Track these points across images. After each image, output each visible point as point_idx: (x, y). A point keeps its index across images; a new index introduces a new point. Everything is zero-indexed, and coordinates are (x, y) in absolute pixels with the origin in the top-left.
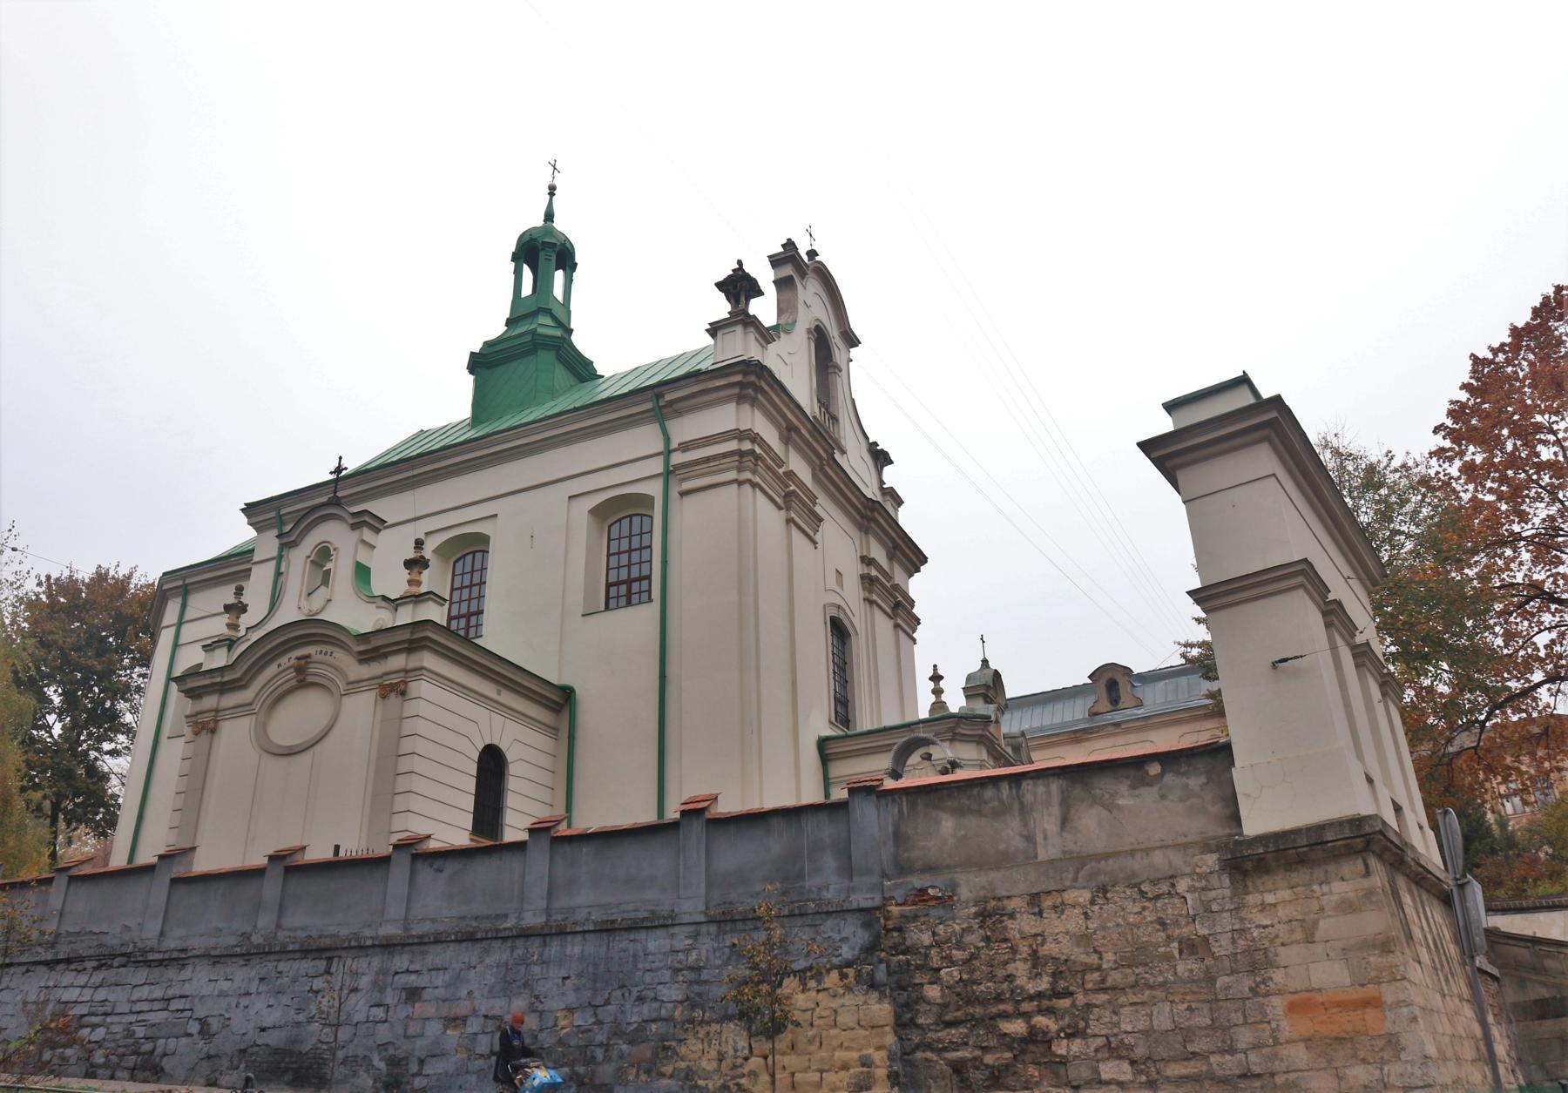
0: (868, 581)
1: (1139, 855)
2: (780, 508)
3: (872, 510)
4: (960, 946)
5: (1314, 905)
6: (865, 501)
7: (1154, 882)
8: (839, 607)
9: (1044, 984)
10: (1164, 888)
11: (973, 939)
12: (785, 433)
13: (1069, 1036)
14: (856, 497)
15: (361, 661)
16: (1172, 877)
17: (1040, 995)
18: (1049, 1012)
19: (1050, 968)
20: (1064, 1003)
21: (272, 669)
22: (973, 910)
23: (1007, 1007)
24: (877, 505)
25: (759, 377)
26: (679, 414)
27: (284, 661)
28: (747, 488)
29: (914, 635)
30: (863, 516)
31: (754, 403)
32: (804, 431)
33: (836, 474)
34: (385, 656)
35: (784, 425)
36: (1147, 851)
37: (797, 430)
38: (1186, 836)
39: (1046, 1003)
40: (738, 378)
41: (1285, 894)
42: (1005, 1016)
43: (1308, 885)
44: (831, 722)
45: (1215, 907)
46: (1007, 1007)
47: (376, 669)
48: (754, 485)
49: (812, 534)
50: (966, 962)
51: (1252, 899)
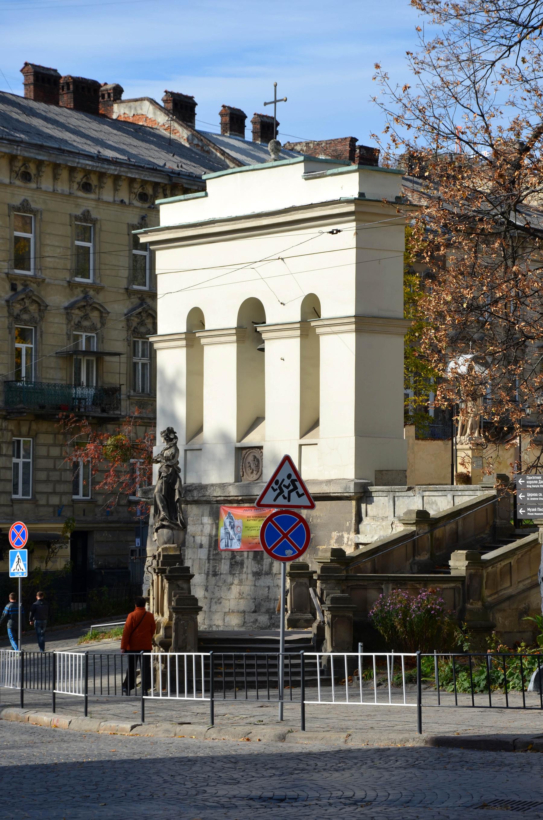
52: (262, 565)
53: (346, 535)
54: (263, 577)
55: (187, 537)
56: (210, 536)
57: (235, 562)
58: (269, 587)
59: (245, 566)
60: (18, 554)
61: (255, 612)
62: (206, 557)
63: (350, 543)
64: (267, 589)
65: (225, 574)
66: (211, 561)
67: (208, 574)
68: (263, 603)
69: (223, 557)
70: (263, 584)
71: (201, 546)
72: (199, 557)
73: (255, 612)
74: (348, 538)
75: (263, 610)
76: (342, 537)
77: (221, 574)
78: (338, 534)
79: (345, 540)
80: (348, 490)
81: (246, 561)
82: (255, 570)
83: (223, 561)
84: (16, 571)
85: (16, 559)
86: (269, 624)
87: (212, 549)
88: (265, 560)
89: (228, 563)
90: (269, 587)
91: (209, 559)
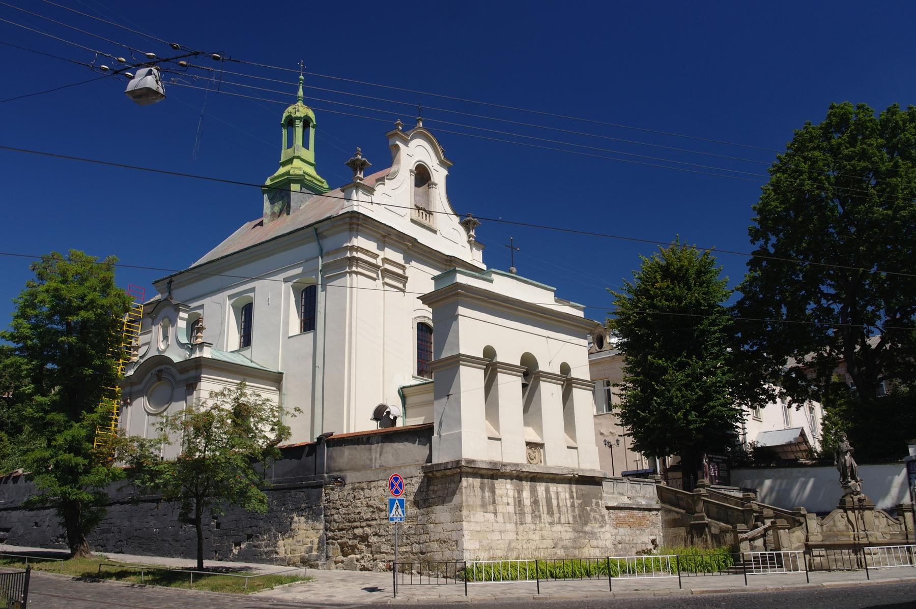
1: (403, 468)
2: (374, 279)
4: (346, 500)
5: (446, 492)
7: (406, 478)
8: (424, 317)
9: (368, 516)
10: (409, 481)
11: (350, 497)
12: (382, 238)
13: (374, 535)
15: (181, 373)
16: (412, 477)
17: (367, 520)
18: (369, 526)
19: (372, 509)
20: (374, 523)
21: (149, 375)
22: (351, 487)
23: (357, 524)
26: (325, 237)
27: (153, 371)
28: (354, 275)
30: (446, 265)
34: (188, 371)
35: (379, 236)
36: (405, 467)
38: (418, 461)
39: (368, 522)
41: (440, 486)
42: (357, 527)
43: (445, 484)
44: (413, 377)
45: (422, 490)
46: (357, 524)
47: (184, 376)
48: (357, 273)
49: (401, 286)
50: (347, 506)
51: (431, 488)
52: (554, 518)
53: (600, 502)
58: (561, 532)
59: (542, 518)
60: (397, 501)
61: (554, 548)
62: (513, 512)
65: (530, 523)
67: (516, 524)
68: (558, 542)
70: (557, 530)
71: (508, 504)
73: (554, 548)
75: (560, 546)
76: (598, 502)
79: (600, 504)
81: (542, 515)
82: (549, 521)
84: (394, 516)
85: (395, 506)
87: (517, 506)
89: (530, 516)
90: (561, 532)
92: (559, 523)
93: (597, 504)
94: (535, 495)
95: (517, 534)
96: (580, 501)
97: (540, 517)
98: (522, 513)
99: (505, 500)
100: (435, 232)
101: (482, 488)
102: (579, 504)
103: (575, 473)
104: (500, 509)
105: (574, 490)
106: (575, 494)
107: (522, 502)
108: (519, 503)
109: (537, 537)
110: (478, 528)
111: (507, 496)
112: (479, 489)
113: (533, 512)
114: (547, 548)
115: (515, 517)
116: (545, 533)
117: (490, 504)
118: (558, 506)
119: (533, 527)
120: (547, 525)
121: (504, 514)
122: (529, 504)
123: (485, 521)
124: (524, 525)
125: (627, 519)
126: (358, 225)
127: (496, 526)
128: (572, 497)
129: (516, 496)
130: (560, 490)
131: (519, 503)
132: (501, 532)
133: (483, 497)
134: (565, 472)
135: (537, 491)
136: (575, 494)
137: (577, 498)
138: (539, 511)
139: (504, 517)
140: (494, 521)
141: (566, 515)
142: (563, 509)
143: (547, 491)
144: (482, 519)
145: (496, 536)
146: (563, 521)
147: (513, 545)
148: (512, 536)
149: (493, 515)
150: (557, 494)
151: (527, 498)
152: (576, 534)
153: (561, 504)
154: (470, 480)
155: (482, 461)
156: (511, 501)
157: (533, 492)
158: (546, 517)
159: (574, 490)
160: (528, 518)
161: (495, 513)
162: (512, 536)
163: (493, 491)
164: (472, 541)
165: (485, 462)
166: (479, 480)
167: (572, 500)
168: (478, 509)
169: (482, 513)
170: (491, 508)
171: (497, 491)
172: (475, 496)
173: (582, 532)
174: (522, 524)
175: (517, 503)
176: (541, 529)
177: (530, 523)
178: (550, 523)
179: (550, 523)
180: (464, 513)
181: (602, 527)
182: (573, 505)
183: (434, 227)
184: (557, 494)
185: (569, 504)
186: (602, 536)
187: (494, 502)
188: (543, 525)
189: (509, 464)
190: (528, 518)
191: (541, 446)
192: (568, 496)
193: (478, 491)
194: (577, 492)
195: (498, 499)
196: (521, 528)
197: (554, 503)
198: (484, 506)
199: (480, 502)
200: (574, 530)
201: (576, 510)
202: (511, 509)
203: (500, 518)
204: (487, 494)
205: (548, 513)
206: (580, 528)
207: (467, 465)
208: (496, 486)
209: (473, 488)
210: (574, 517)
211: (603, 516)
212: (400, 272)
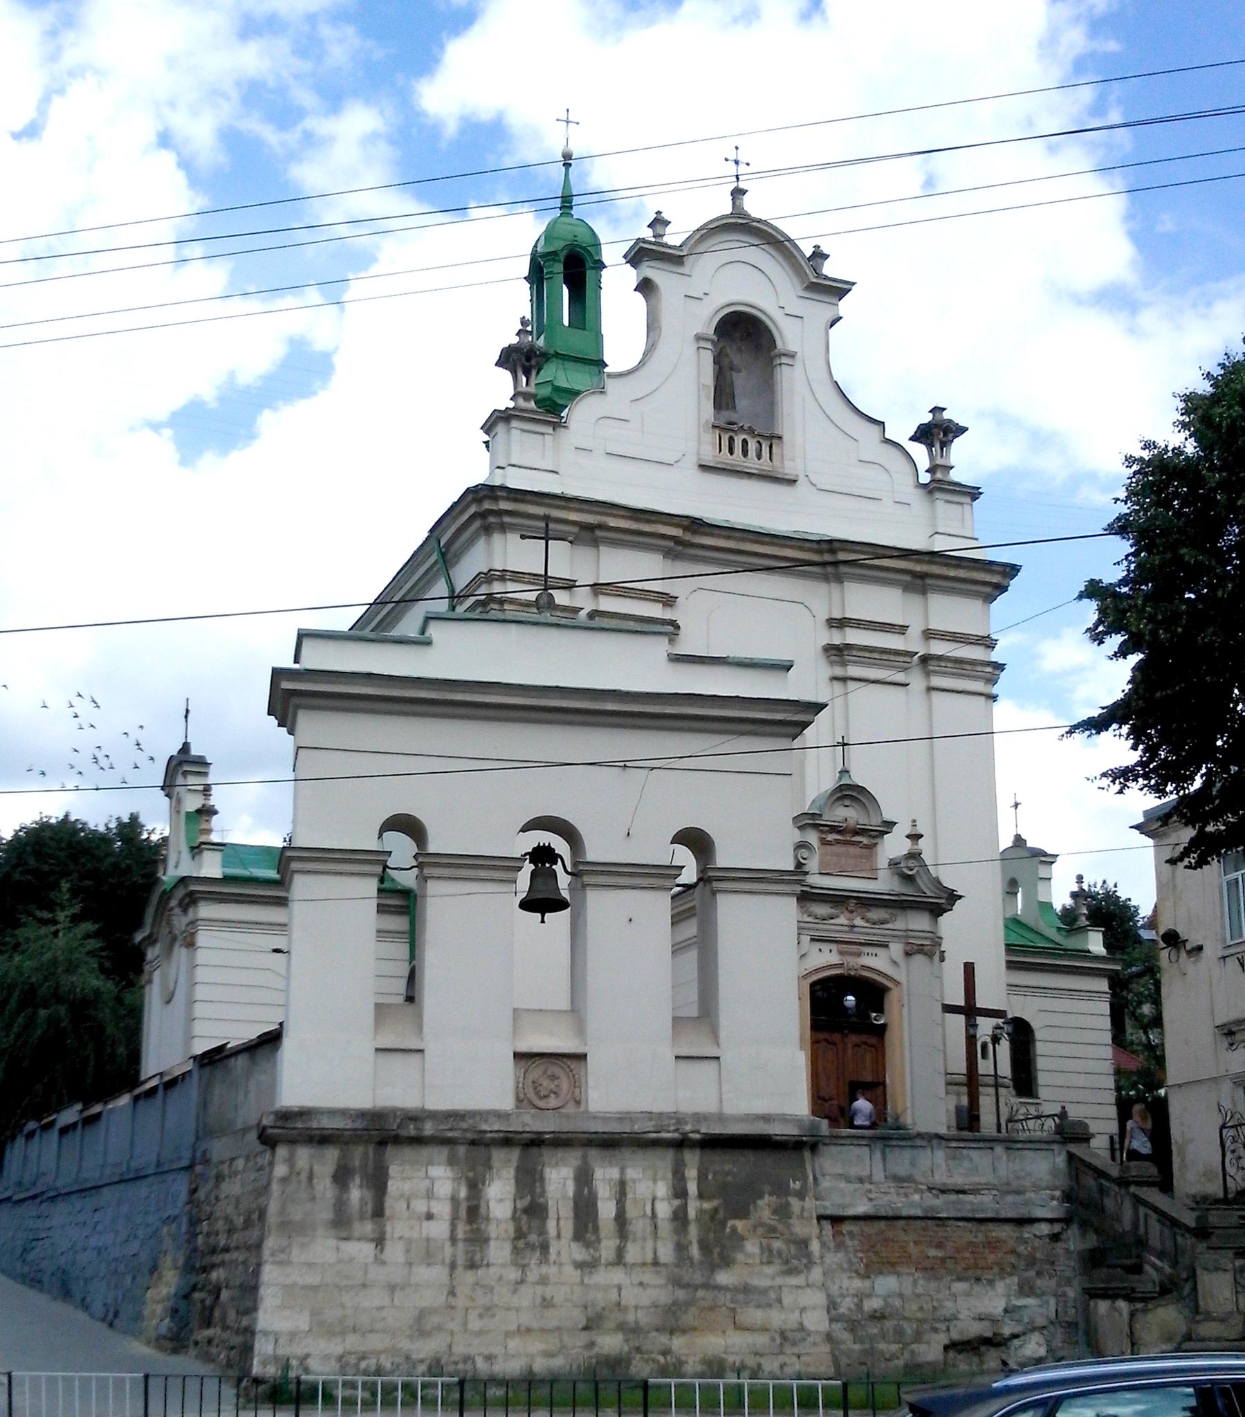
0: (837, 653)
3: (833, 551)
6: (815, 546)
14: (792, 547)
24: (837, 545)
25: (496, 499)
29: (995, 690)
31: (503, 528)
32: (613, 522)
33: (729, 538)
37: (600, 527)
40: (473, 509)
53: (795, 1203)
54: (602, 1269)
55: (389, 1202)
56: (454, 1200)
57: (527, 1244)
61: (586, 1328)
63: (806, 1214)
64: (615, 1290)
65: (503, 1265)
66: (461, 1245)
67: (453, 1266)
68: (606, 1313)
69: (493, 1235)
71: (430, 1216)
72: (424, 1235)
74: (803, 1208)
75: (612, 1325)
76: (788, 1204)
77: (488, 1265)
78: (779, 1200)
80: (815, 1133)
83: (492, 1243)
86: (626, 1349)
88: (604, 1243)
89: (508, 1247)
91: (453, 1239)
92: (619, 1259)
93: (783, 1212)
94: (532, 1193)
95: (452, 1293)
96: (707, 1205)
97: (545, 1248)
98: (478, 1239)
99: (420, 1206)
100: (792, 482)
101: (341, 1177)
102: (701, 1212)
103: (688, 1128)
104: (397, 1228)
105: (691, 1173)
106: (692, 1188)
107: (483, 1210)
108: (473, 1212)
109: (526, 1297)
110: (312, 1279)
111: (430, 1195)
112: (328, 1181)
113: (520, 1235)
114: (558, 1329)
115: (448, 1250)
116: (558, 1293)
117: (362, 1218)
118: (621, 1219)
119: (513, 1274)
120: (569, 1270)
121: (409, 1242)
122: (509, 1214)
123: (339, 1261)
124: (480, 1272)
125: (912, 1249)
126: (500, 513)
127: (377, 1273)
128: (680, 1192)
129: (463, 1193)
130: (631, 1173)
131: (473, 1212)
132: (392, 1288)
133: (340, 1206)
134: (649, 1125)
135: (542, 1179)
136: (692, 1188)
137: (701, 1196)
138: (542, 1232)
139: (408, 1251)
140: (371, 1259)
141: (649, 1245)
142: (639, 1226)
143: (584, 1178)
144: (331, 1257)
145: (373, 1299)
146: (633, 1253)
147: (435, 1320)
148: (432, 1298)
149: (368, 1249)
150: (622, 1189)
151: (501, 1200)
152: (681, 1294)
153: (631, 1212)
154: (303, 1155)
155: (332, 1112)
156: (443, 1209)
157: (529, 1180)
158: (566, 1249)
159: (691, 1173)
160: (499, 1251)
161: (380, 1241)
162: (432, 1298)
163: (378, 1184)
164: (287, 1312)
165: (343, 1112)
166: (332, 1155)
167: (677, 1202)
168: (320, 1231)
169: (332, 1242)
170: (368, 1227)
171: (393, 1186)
172: (313, 1199)
173: (706, 1286)
174: (472, 1265)
175: (463, 1213)
176: (544, 1281)
177: (503, 1265)
178: (579, 1265)
179: (585, 1266)
180: (270, 1243)
181: (790, 1272)
182: (679, 1217)
183: (789, 469)
184: (622, 1189)
185: (664, 1210)
186: (787, 1299)
187: (379, 1212)
188: (551, 1270)
189: (433, 1115)
190: (499, 1251)
191: (582, 1057)
192: (662, 1189)
193: (325, 1187)
194: (702, 1177)
195: (393, 1204)
196: (469, 1277)
197: (606, 1210)
198: (341, 1222)
199: (328, 1215)
200: (677, 1282)
201: (693, 1232)
202: (439, 1230)
203: (395, 1252)
204: (356, 1194)
205: (579, 1236)
206: (698, 1278)
207: (279, 1124)
208: (393, 1170)
209: (311, 1178)
210: (681, 1248)
211: (804, 1243)
212: (653, 610)
